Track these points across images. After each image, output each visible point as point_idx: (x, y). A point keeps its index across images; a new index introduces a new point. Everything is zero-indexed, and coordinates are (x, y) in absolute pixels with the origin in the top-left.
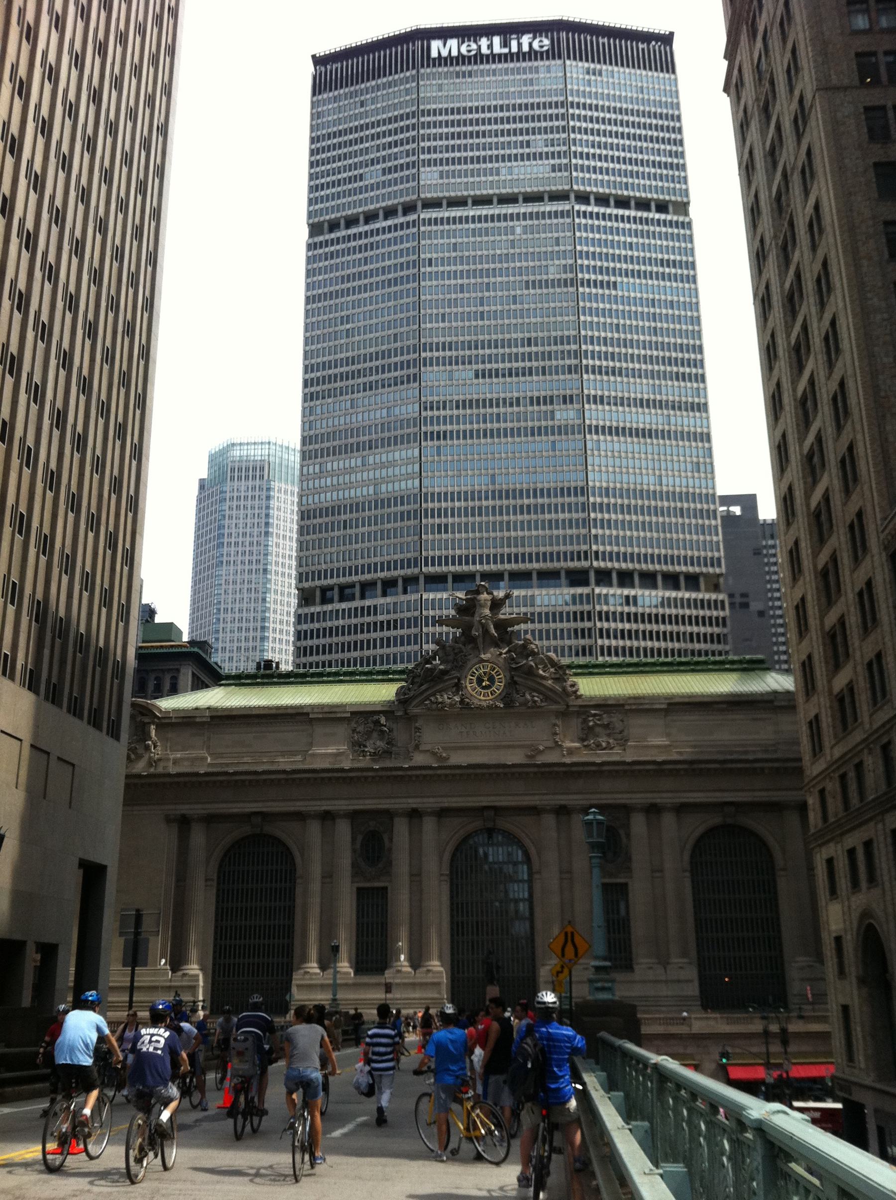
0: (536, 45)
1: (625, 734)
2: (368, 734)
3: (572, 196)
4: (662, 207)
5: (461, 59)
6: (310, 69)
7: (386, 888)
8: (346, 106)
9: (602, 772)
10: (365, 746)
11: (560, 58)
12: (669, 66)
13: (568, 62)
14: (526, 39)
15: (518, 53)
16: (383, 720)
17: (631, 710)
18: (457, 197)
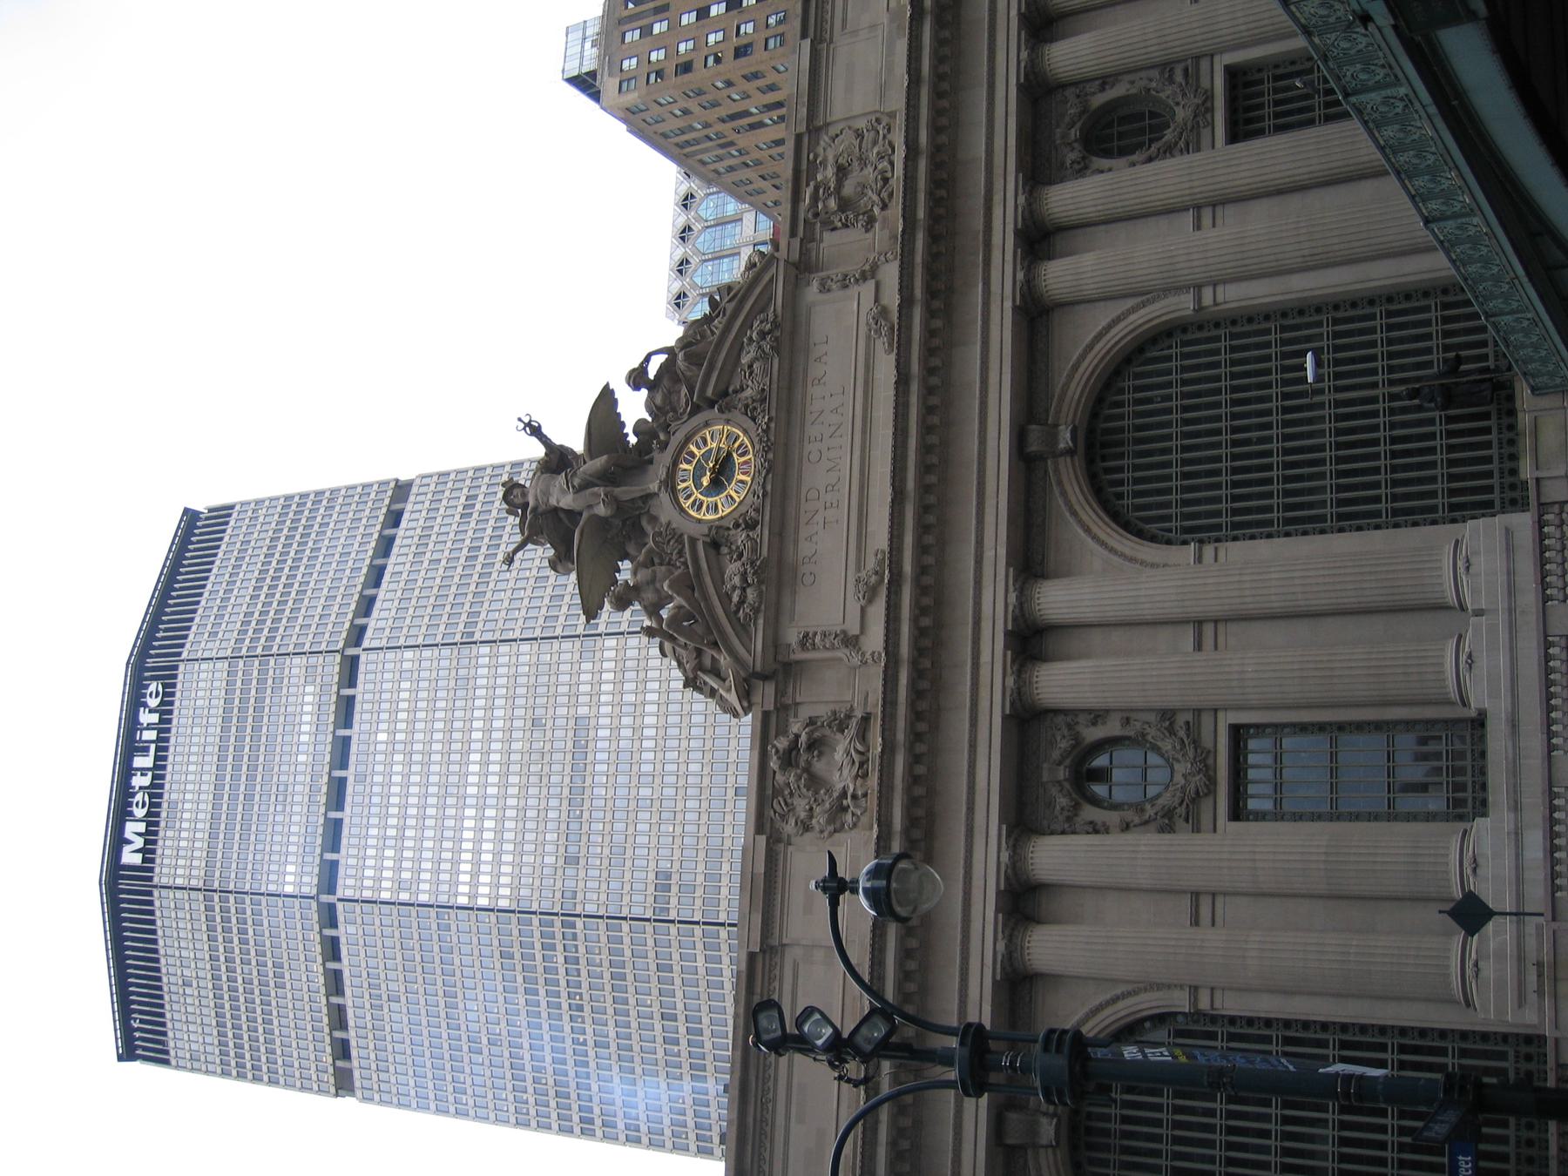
0: (153, 702)
1: (861, 124)
2: (815, 782)
3: (351, 651)
4: (394, 518)
5: (152, 820)
6: (137, 1065)
7: (1238, 734)
8: (187, 1013)
9: (936, 149)
10: (844, 794)
11: (176, 668)
12: (222, 514)
13: (184, 655)
14: (146, 718)
15: (160, 731)
16: (782, 743)
17: (811, 116)
18: (323, 836)
